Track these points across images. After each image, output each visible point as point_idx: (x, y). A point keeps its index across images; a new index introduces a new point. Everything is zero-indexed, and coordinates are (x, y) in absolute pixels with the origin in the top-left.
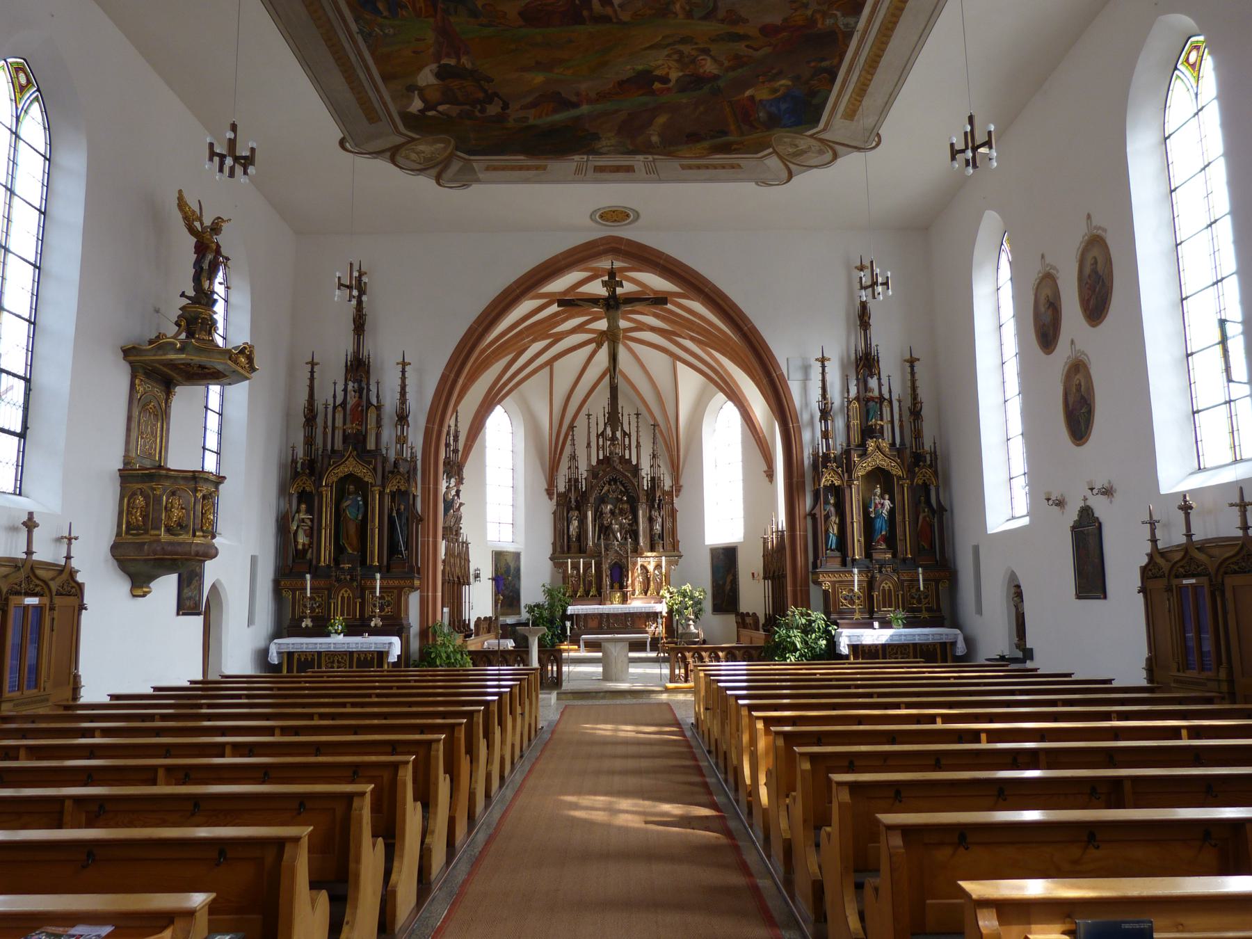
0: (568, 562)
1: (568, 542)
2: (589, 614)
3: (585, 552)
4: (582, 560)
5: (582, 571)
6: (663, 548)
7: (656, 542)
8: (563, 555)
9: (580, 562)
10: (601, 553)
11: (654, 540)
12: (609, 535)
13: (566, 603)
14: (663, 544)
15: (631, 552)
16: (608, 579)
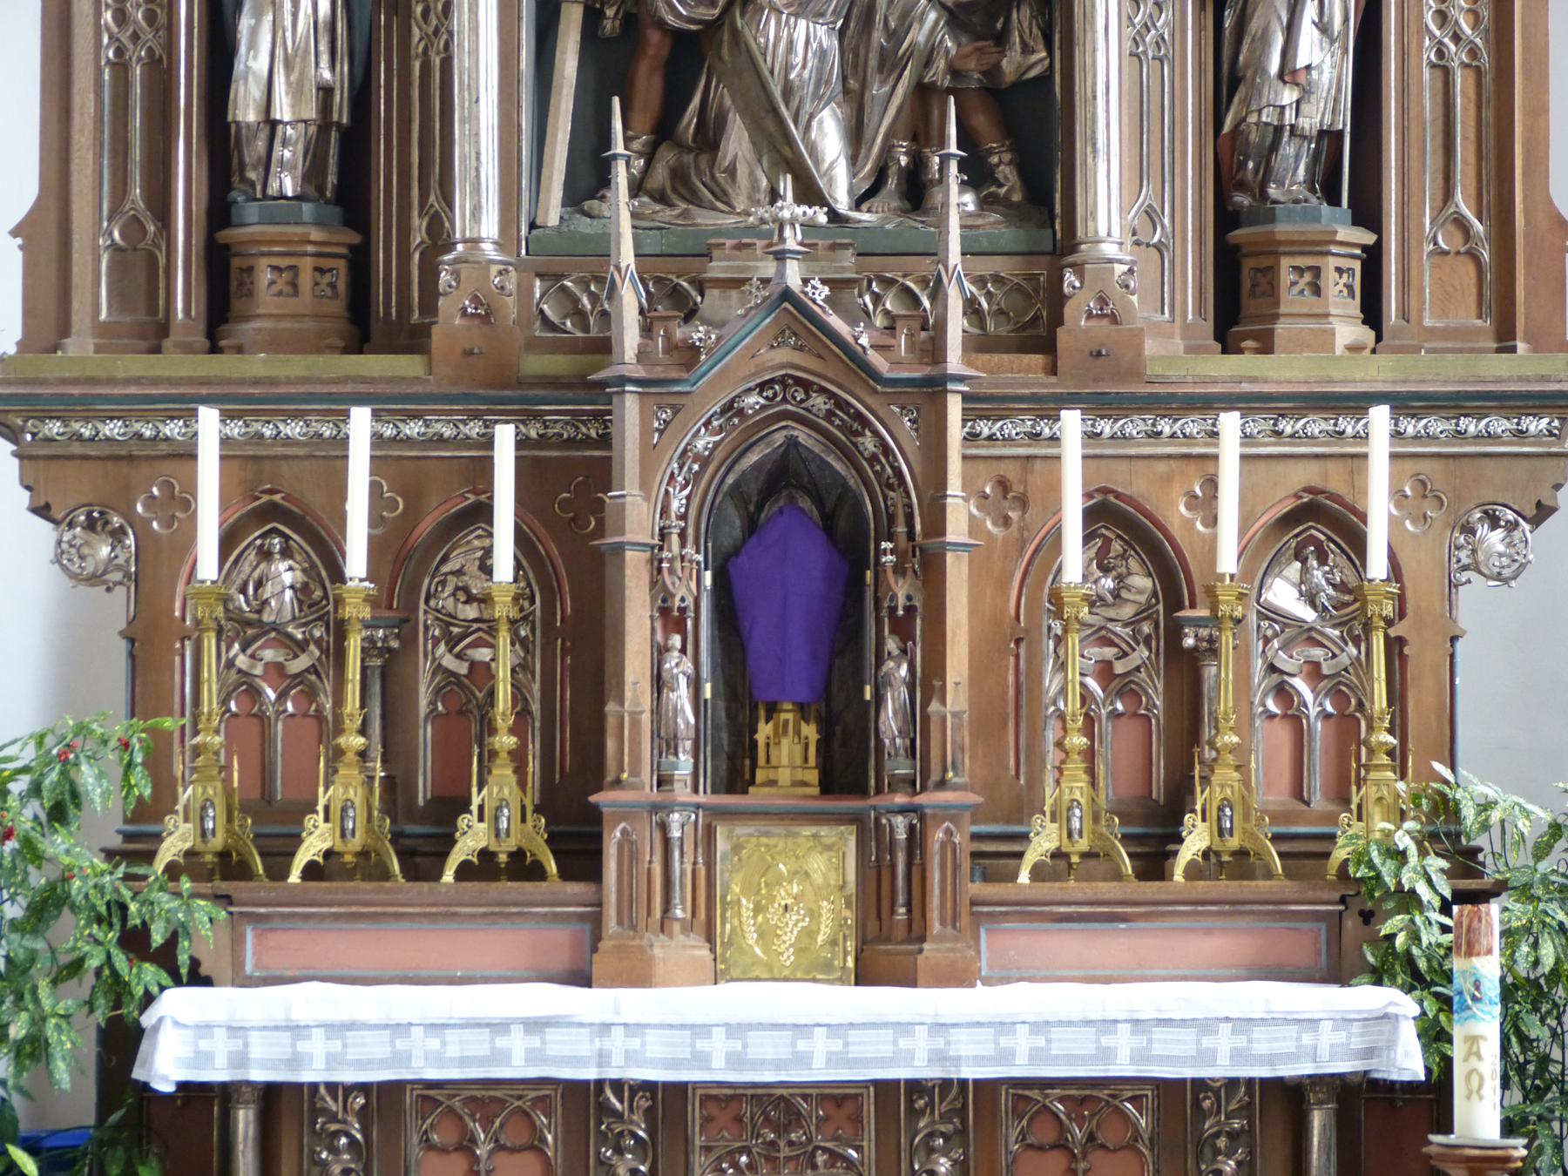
0: (188, 454)
1: (219, 212)
2: (432, 1094)
3: (413, 339)
4: (360, 422)
5: (356, 563)
6: (1372, 313)
7: (1283, 229)
8: (136, 364)
9: (342, 442)
10: (604, 347)
11: (1265, 212)
12: (709, 139)
13: (135, 941)
14: (1372, 259)
15: (978, 344)
16: (678, 666)
